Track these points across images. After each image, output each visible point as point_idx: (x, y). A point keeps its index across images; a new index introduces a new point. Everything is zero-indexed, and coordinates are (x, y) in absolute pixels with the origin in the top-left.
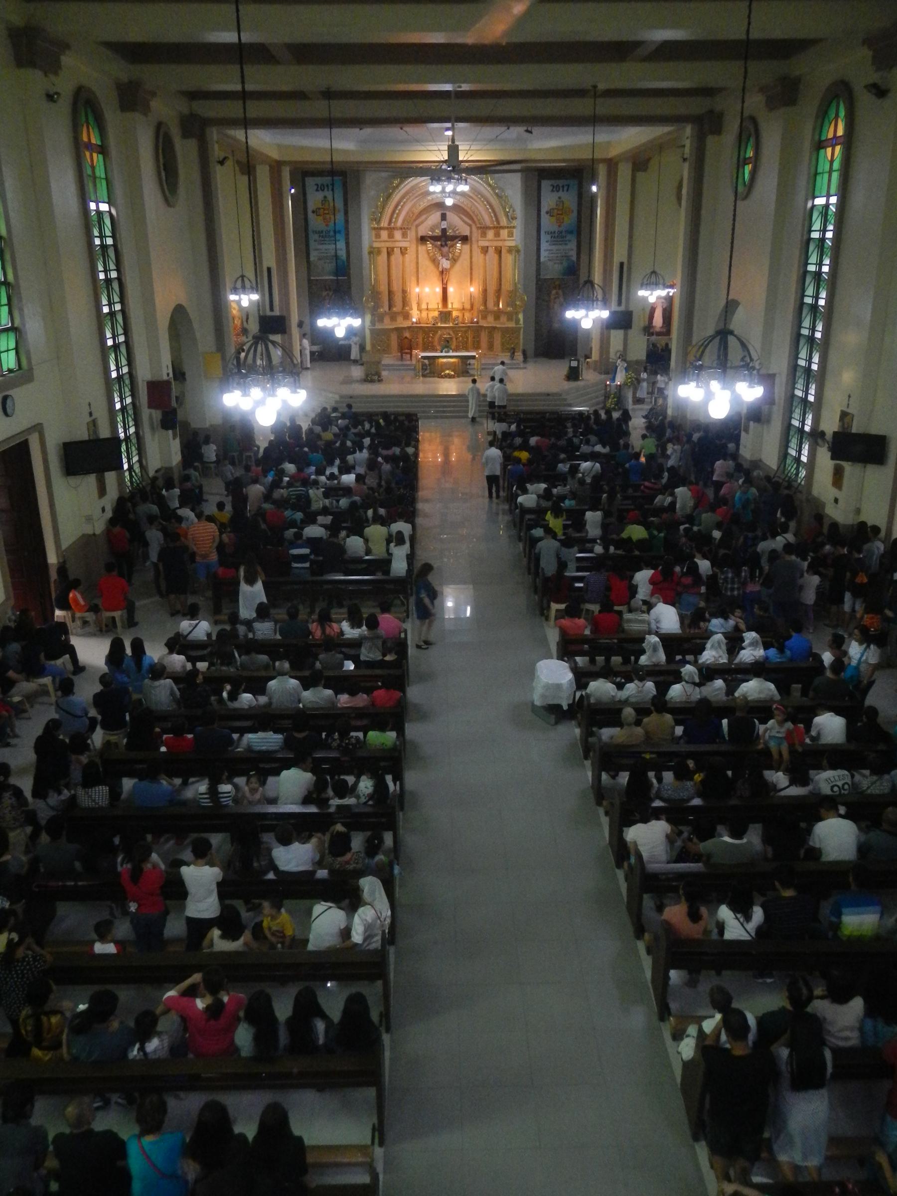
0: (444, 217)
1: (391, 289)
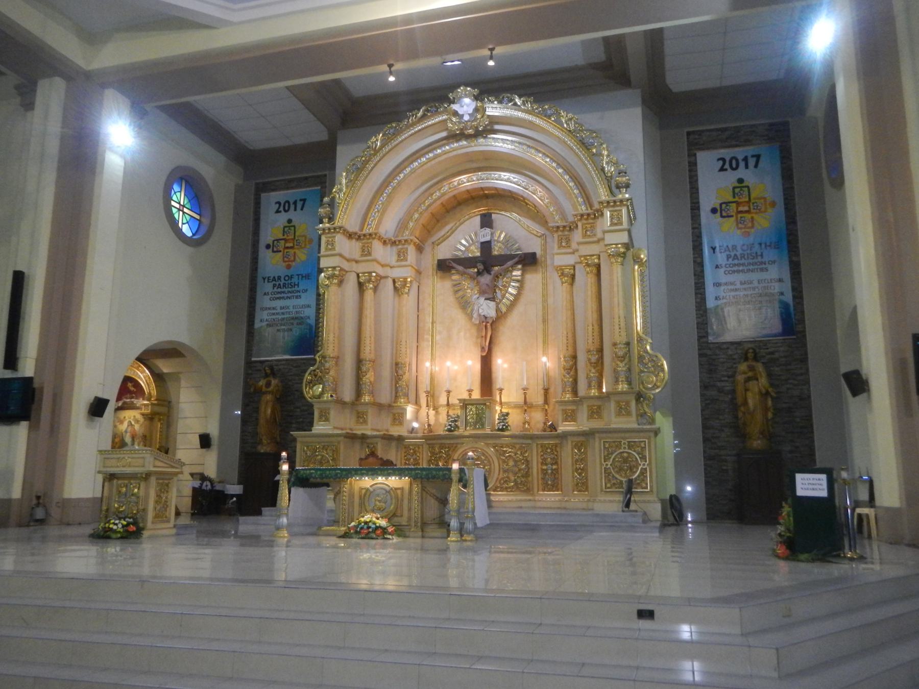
0: (487, 222)
1: (362, 356)
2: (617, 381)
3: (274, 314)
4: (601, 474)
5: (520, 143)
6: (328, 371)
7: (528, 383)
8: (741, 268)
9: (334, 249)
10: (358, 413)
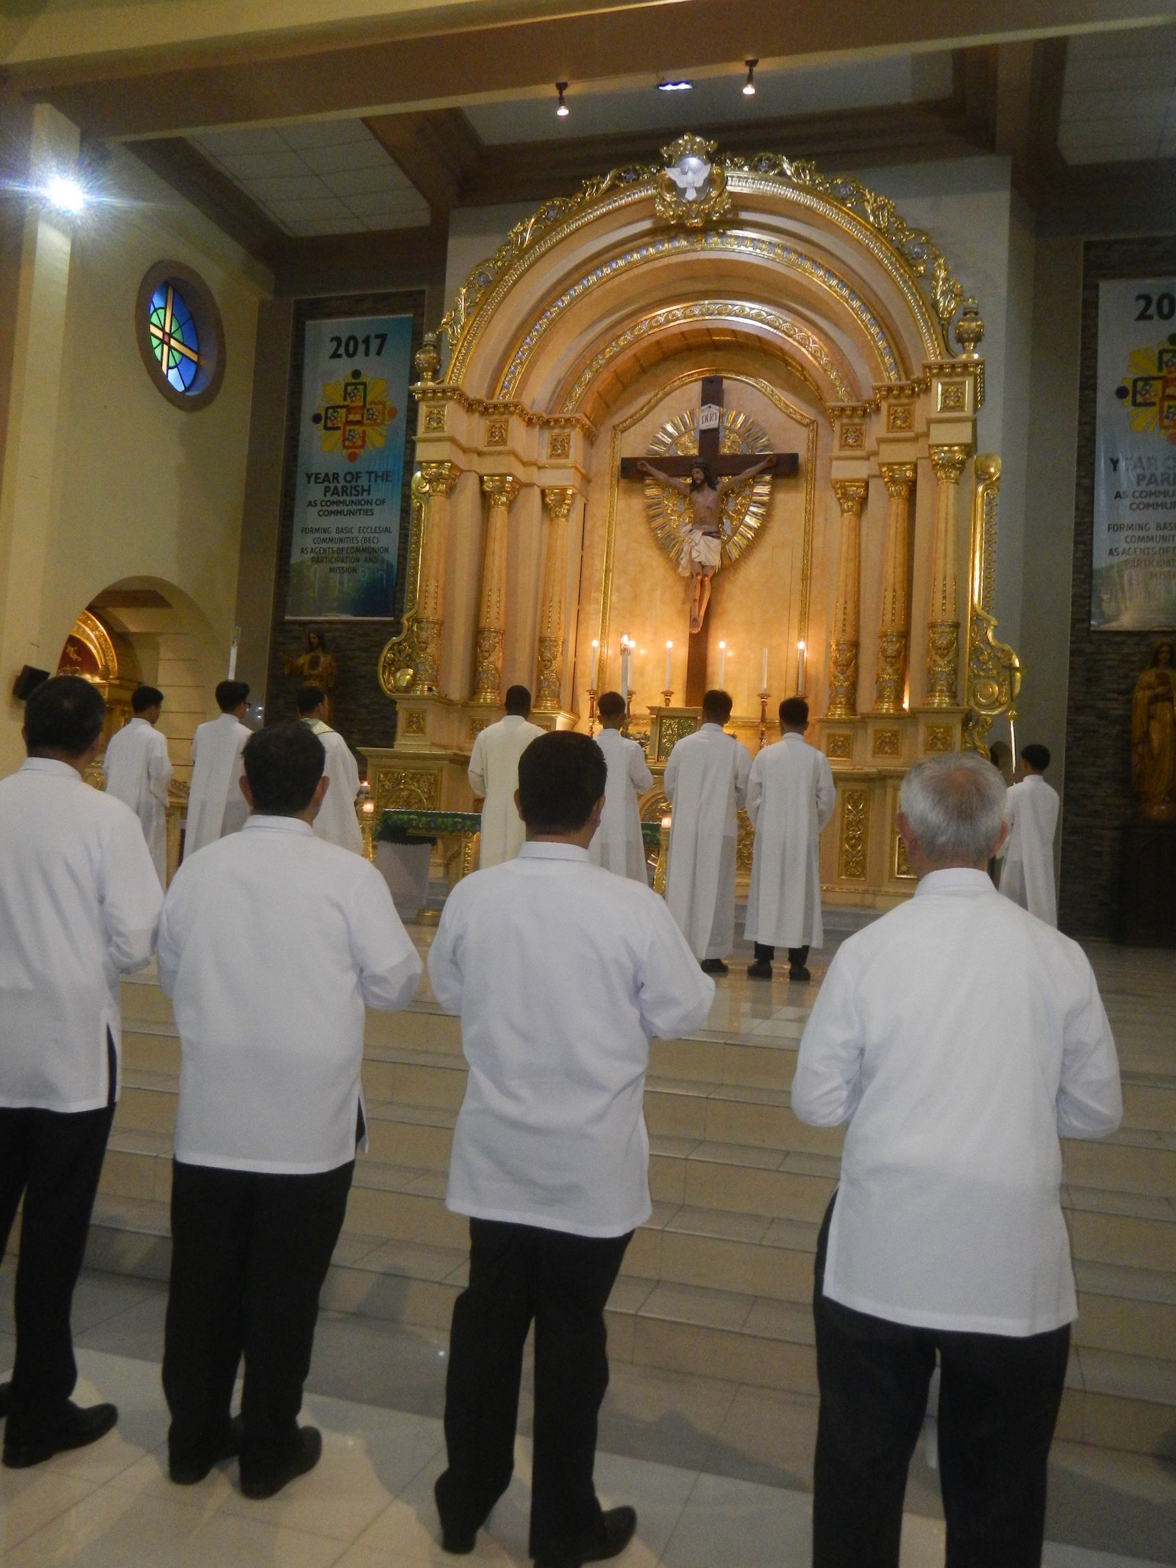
0: (713, 393)
1: (484, 623)
2: (931, 691)
3: (324, 540)
4: (893, 848)
5: (784, 248)
6: (424, 645)
7: (770, 686)
8: (1160, 500)
9: (440, 428)
10: (474, 721)
